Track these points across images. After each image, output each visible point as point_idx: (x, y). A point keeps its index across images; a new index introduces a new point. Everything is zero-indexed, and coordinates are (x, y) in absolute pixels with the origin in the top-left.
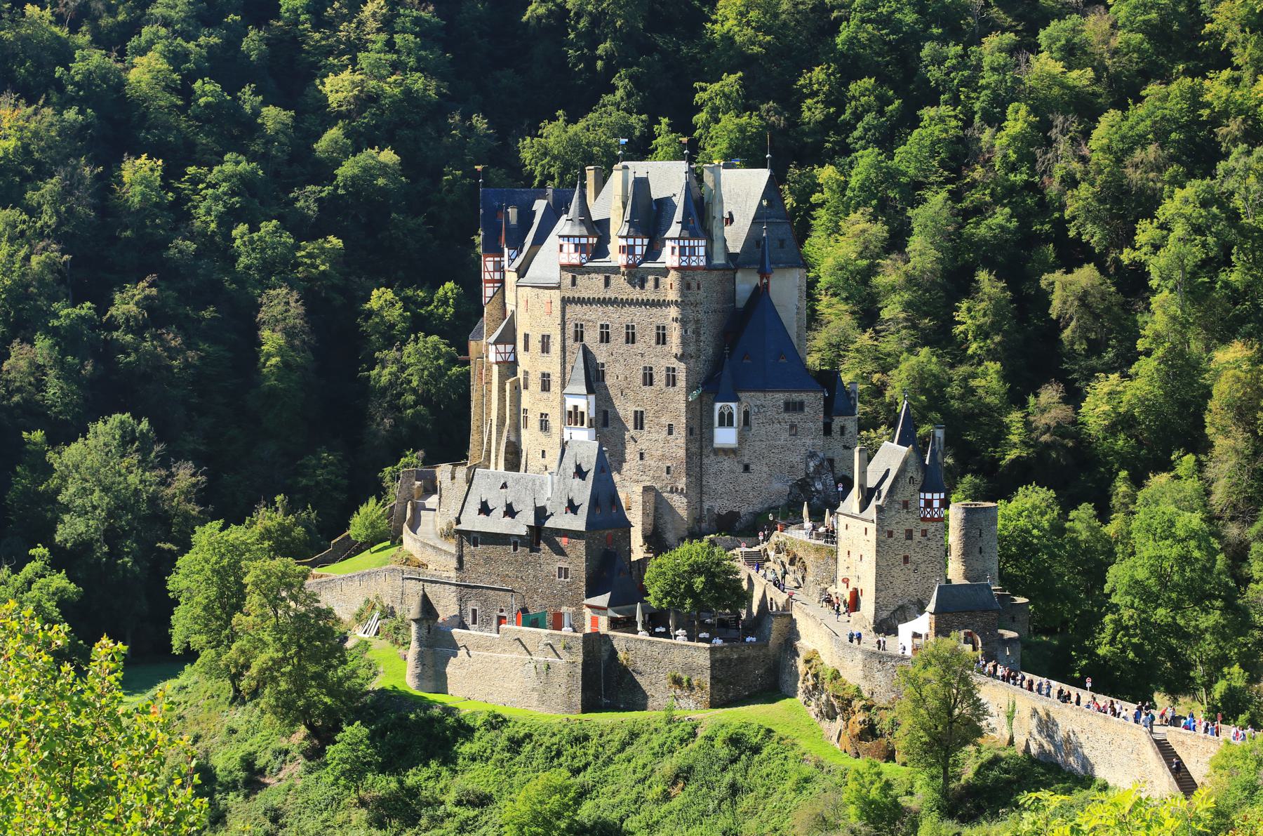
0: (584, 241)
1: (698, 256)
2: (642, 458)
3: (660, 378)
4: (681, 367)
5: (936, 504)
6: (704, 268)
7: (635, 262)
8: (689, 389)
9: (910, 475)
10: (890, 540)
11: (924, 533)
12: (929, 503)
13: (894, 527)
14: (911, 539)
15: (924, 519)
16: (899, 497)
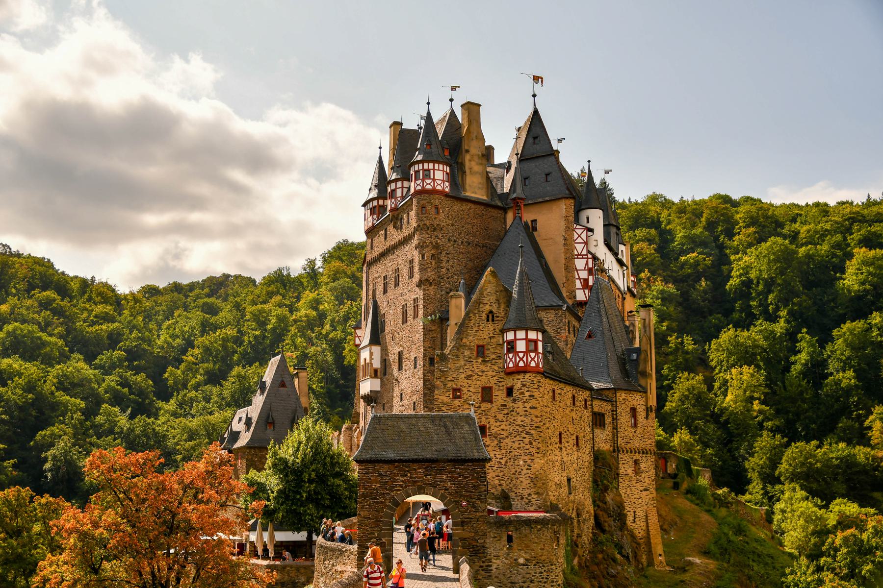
0: (375, 203)
1: (434, 180)
2: (401, 400)
3: (410, 312)
4: (419, 293)
5: (521, 346)
6: (447, 195)
7: (396, 204)
8: (425, 316)
9: (487, 308)
10: (457, 402)
11: (510, 391)
12: (512, 346)
13: (462, 382)
14: (491, 401)
15: (510, 373)
16: (472, 340)
